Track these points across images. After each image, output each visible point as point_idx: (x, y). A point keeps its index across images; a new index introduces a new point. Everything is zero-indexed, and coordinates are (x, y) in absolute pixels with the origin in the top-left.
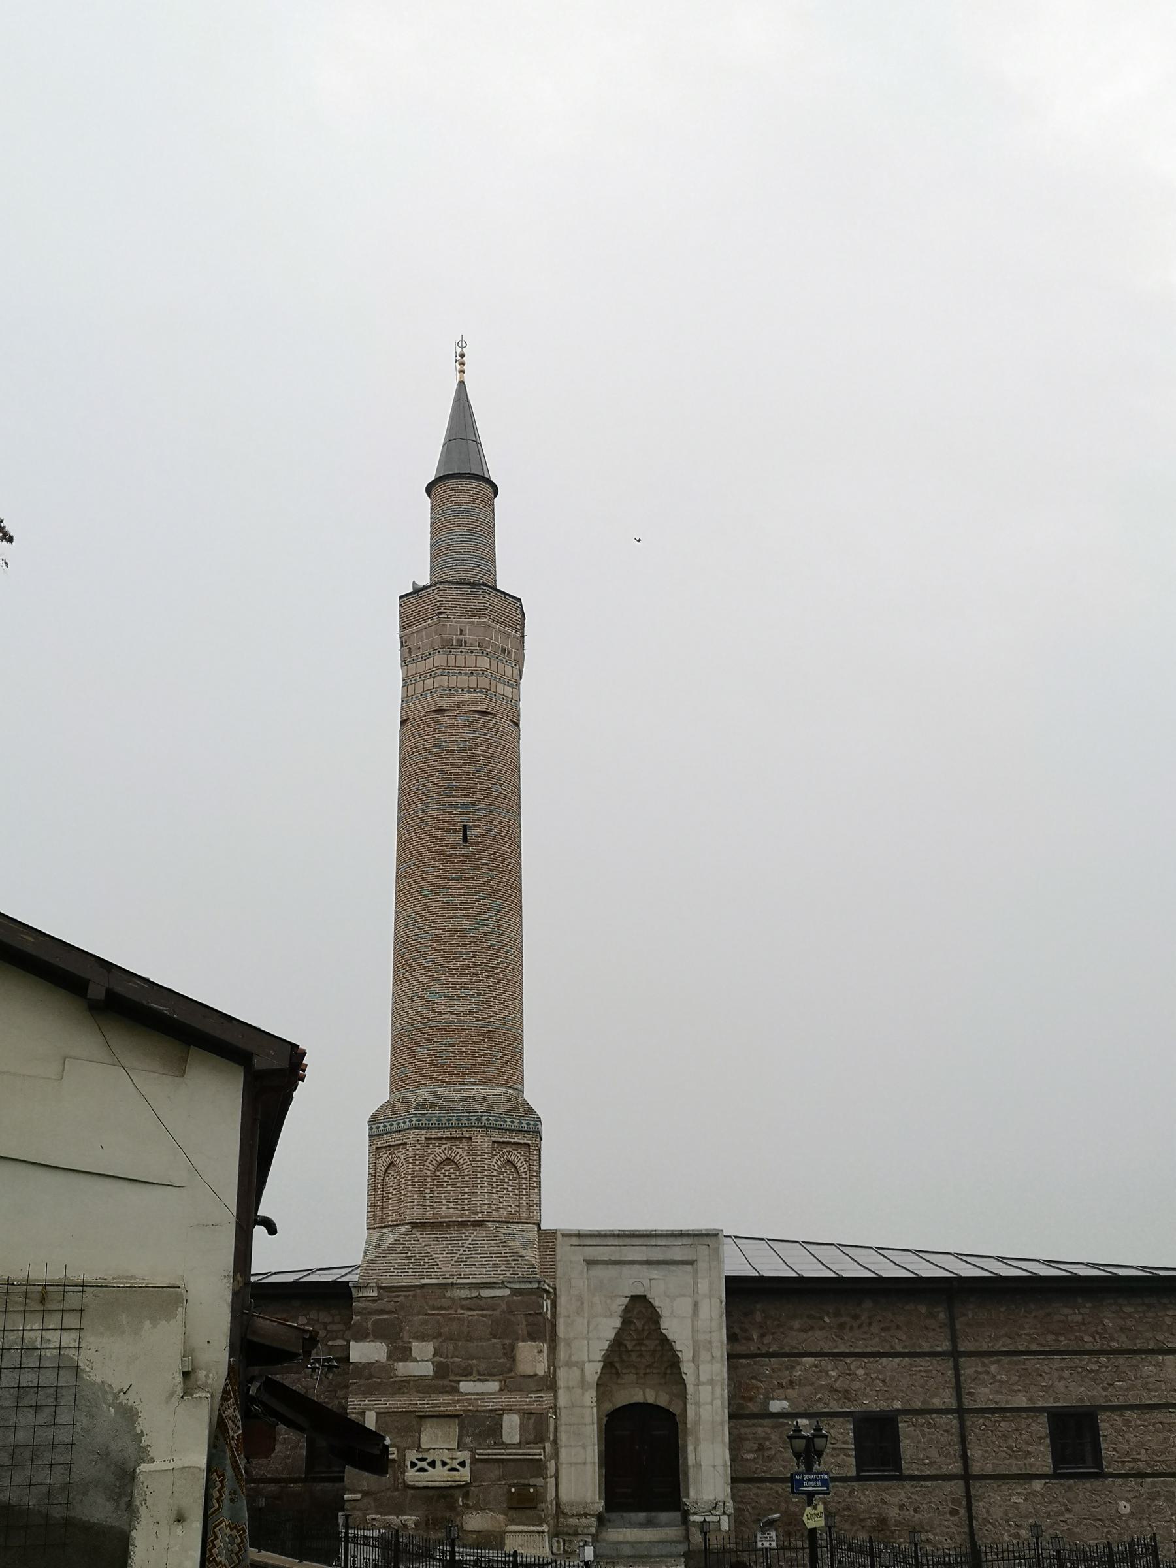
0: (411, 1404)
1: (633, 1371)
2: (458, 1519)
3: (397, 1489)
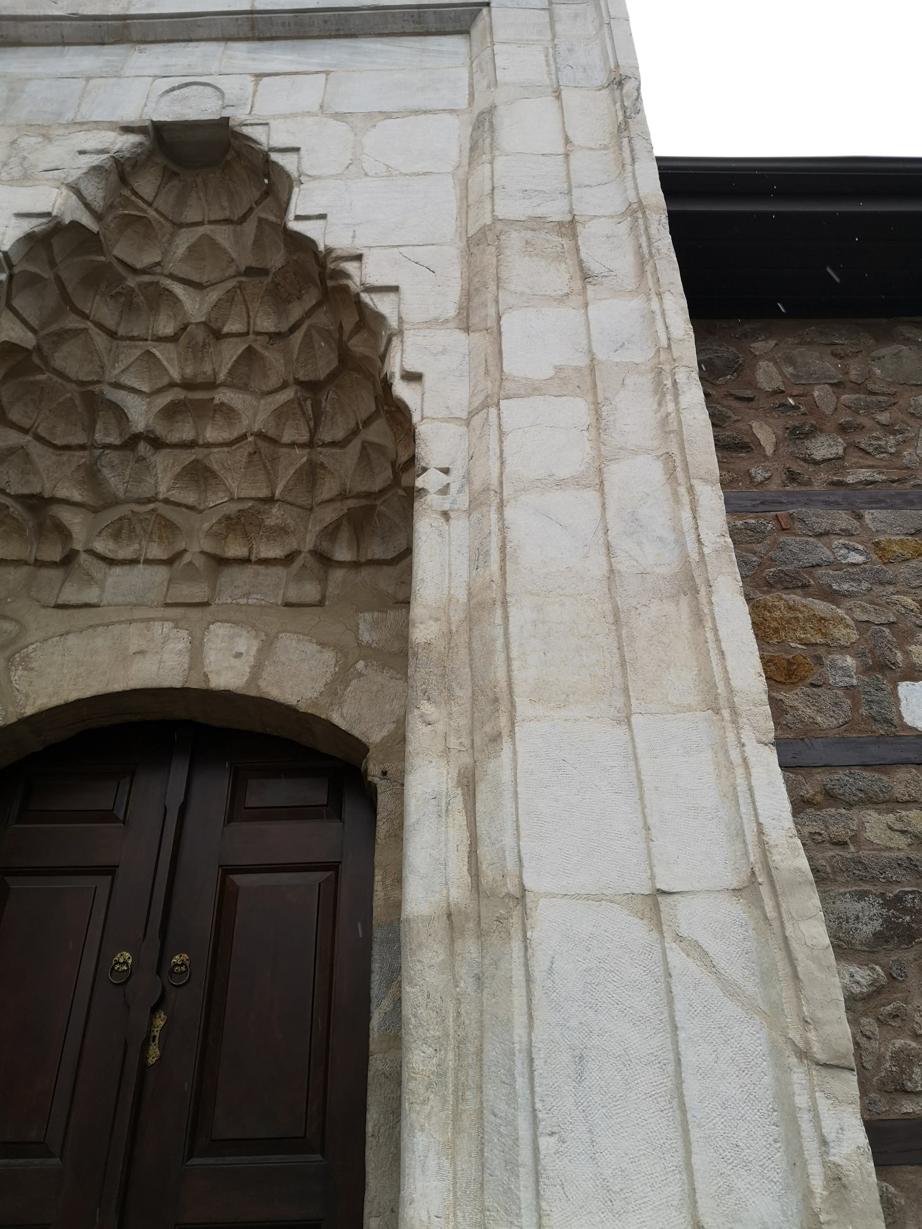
1: (156, 551)
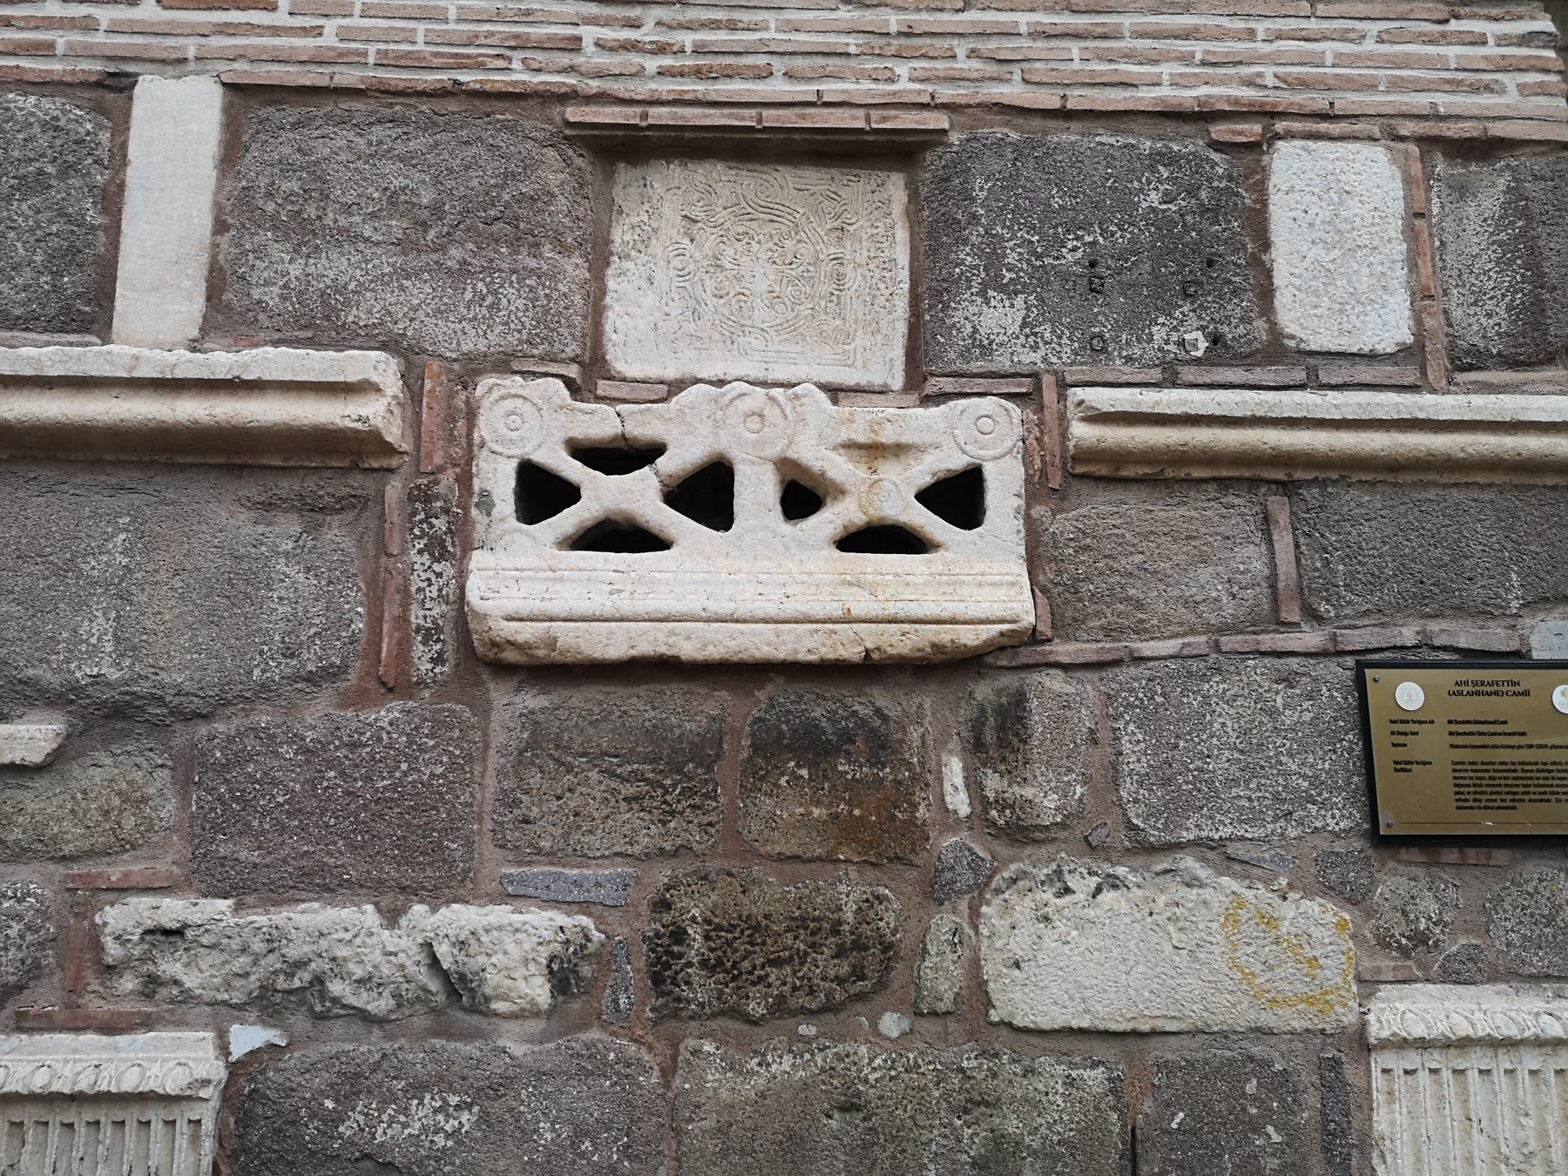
0: (521, 44)
2: (943, 923)
3: (397, 686)
